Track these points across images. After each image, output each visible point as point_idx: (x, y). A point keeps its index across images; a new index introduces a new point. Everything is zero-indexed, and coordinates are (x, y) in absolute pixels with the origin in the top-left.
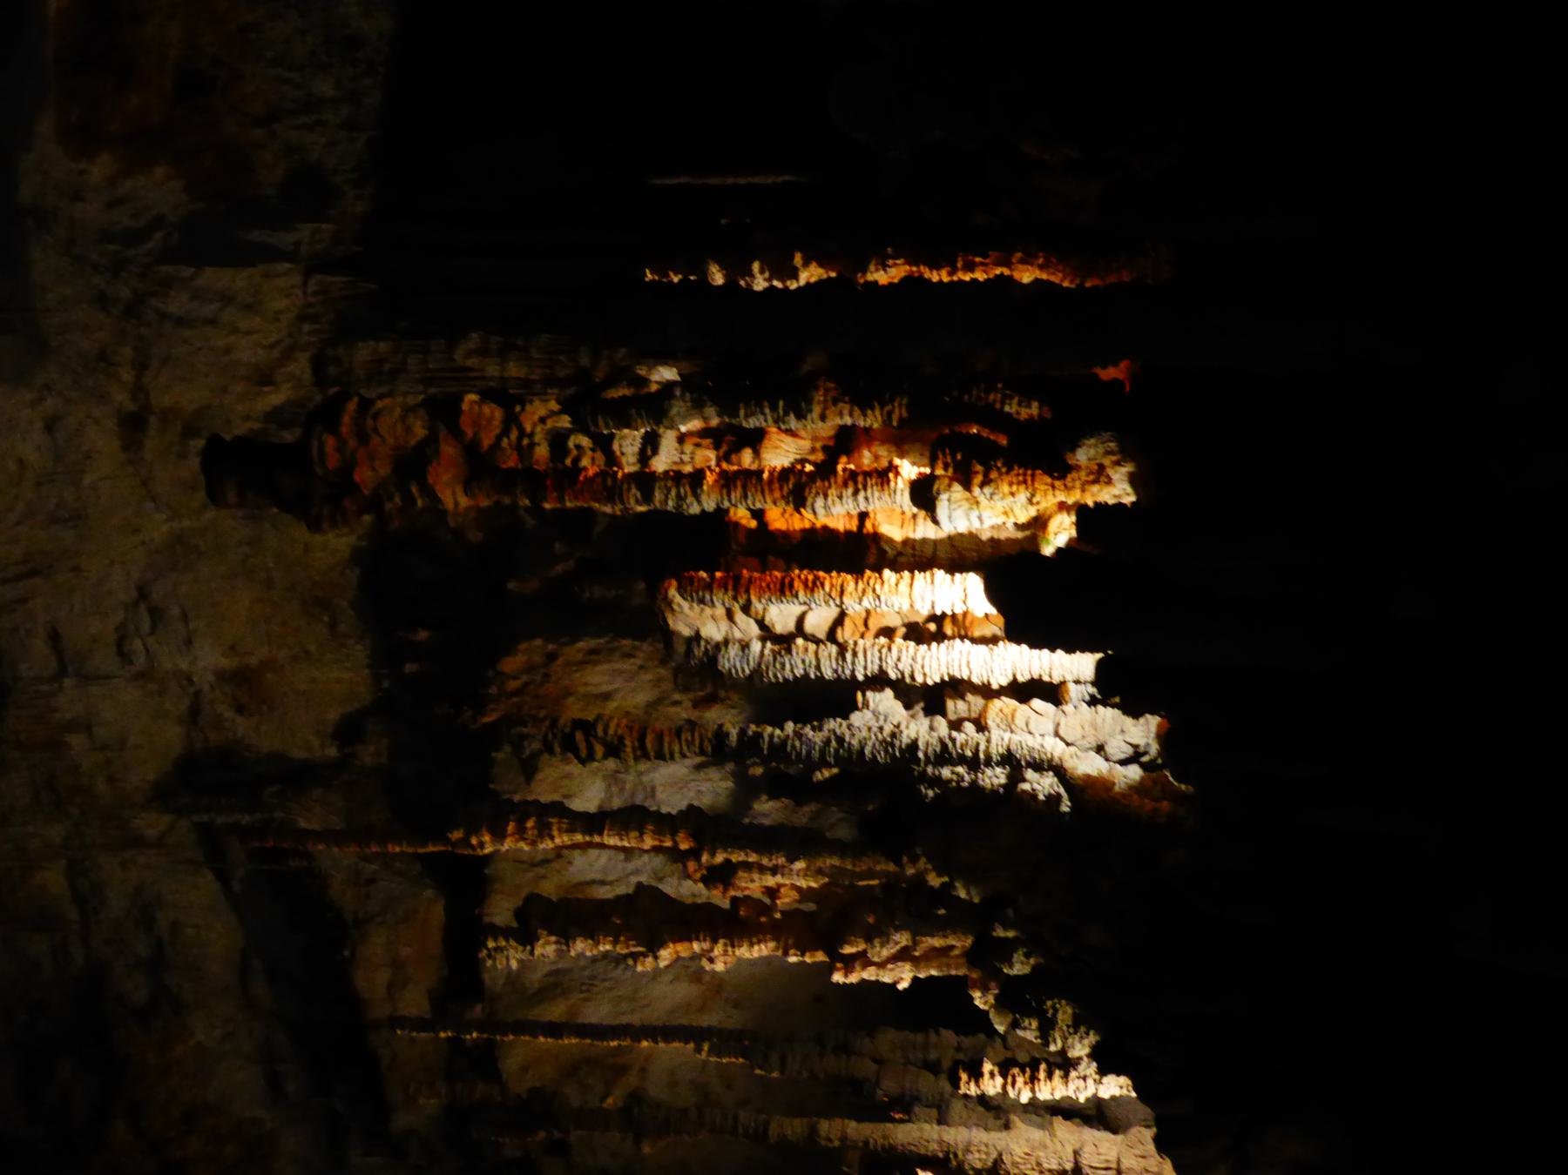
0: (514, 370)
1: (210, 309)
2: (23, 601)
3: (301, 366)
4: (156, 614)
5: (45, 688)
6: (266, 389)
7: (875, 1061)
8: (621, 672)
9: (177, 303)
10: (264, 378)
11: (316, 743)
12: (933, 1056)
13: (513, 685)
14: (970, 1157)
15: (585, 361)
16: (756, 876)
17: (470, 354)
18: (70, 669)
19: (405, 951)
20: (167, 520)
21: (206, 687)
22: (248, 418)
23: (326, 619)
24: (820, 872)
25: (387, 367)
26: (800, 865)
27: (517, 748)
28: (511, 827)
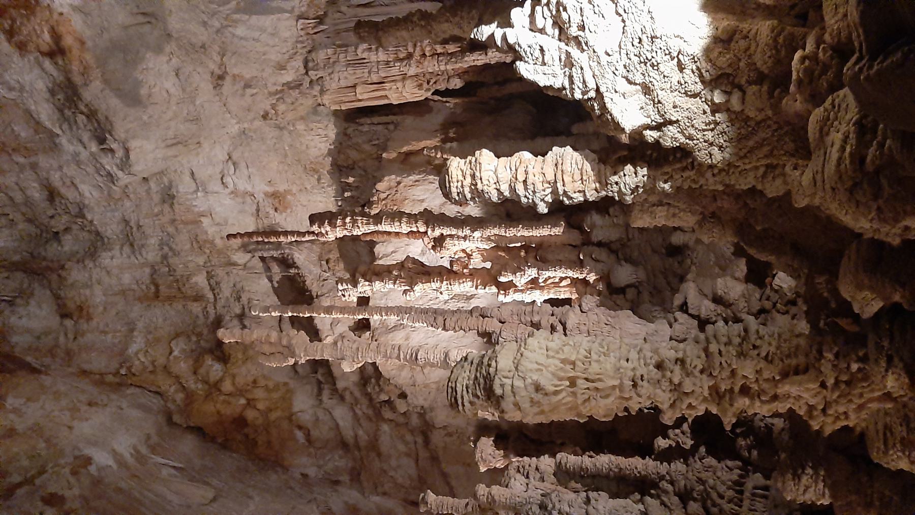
1: (256, 34)
2: (176, 156)
3: (298, 63)
4: (234, 164)
5: (189, 197)
7: (501, 322)
8: (428, 190)
9: (240, 31)
10: (282, 67)
12: (536, 319)
13: (383, 196)
15: (411, 50)
16: (456, 242)
17: (364, 51)
20: (237, 123)
21: (261, 201)
22: (275, 84)
23: (316, 177)
24: (489, 239)
25: (331, 60)
26: (477, 234)
28: (339, 222)
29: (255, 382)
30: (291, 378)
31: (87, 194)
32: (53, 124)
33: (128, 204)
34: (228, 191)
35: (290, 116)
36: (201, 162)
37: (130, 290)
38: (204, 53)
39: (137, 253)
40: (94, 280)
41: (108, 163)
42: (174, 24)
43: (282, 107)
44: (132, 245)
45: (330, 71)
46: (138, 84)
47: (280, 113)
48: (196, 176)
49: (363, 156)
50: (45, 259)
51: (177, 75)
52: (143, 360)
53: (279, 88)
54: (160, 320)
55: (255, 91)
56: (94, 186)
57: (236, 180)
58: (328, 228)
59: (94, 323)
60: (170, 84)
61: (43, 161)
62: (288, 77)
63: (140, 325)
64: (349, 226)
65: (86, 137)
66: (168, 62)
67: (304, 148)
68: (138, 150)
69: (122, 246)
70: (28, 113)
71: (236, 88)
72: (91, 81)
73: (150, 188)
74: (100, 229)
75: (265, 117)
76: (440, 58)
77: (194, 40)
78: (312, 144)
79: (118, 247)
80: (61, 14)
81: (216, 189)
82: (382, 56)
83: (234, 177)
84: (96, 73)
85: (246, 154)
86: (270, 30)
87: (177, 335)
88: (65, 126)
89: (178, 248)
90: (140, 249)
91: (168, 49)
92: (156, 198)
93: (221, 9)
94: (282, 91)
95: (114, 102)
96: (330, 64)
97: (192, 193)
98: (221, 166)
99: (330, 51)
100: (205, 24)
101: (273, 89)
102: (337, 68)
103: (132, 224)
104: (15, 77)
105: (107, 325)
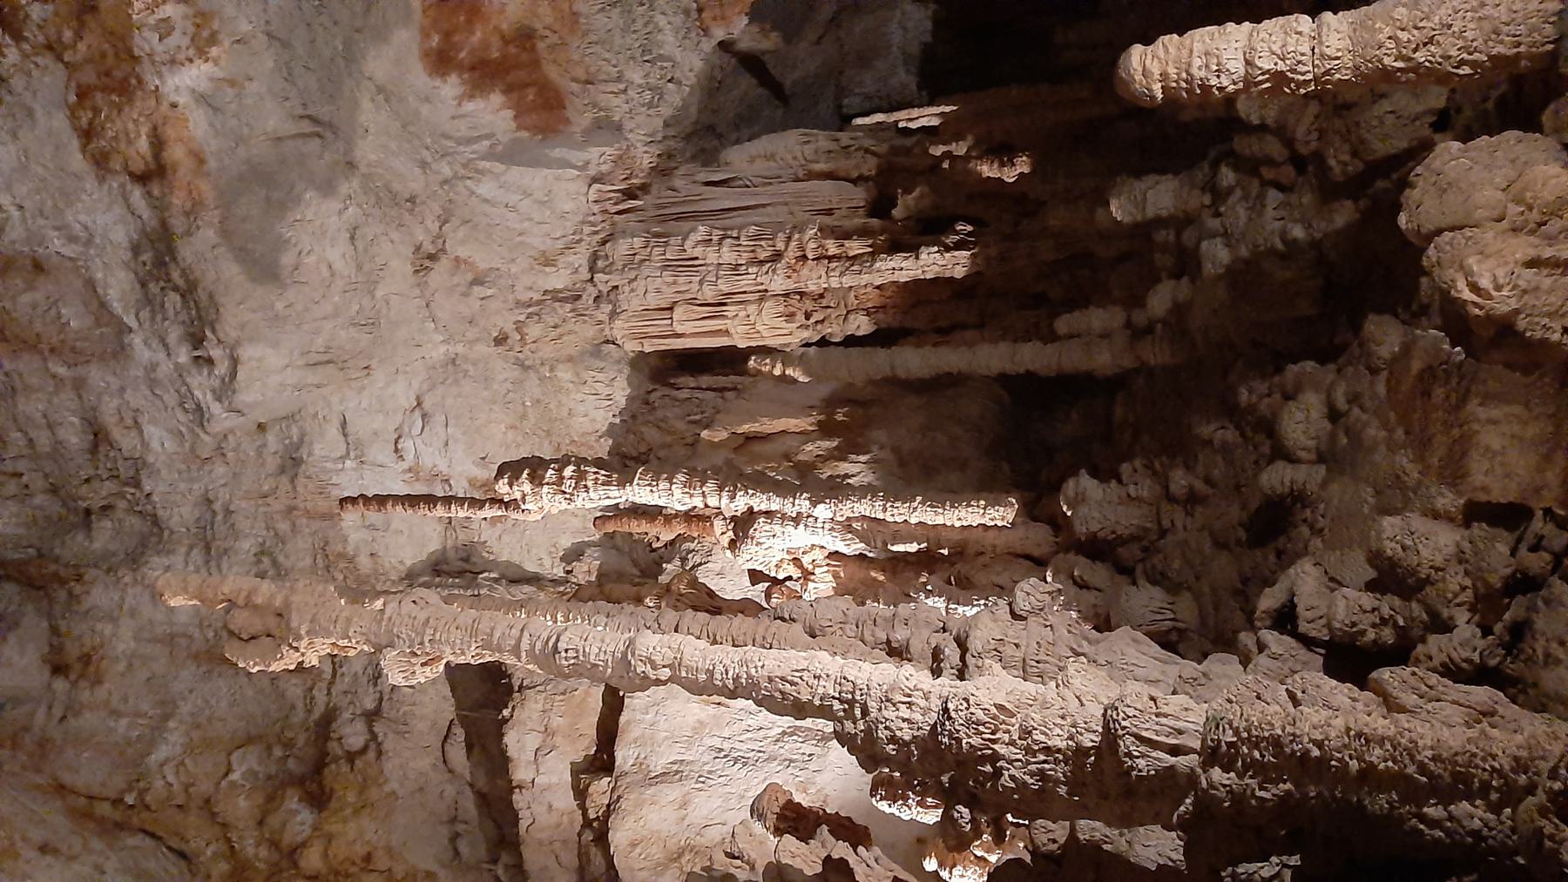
0: (728, 255)
1: (513, 198)
3: (580, 258)
4: (424, 416)
6: (547, 269)
9: (486, 188)
10: (547, 261)
11: (547, 563)
12: (900, 635)
14: (889, 713)
15: (780, 246)
16: (777, 528)
18: (352, 455)
19: (556, 722)
24: (847, 526)
26: (823, 511)
27: (684, 560)
29: (368, 858)
30: (443, 866)
31: (155, 445)
32: (125, 308)
33: (220, 469)
34: (405, 465)
35: (547, 351)
36: (364, 405)
37: (184, 635)
38: (411, 211)
39: (213, 563)
40: (125, 608)
41: (201, 385)
42: (367, 151)
43: (534, 331)
44: (208, 548)
45: (632, 275)
46: (282, 244)
47: (529, 339)
48: (350, 429)
49: (668, 439)
50: (57, 560)
51: (352, 238)
52: (171, 778)
53: (537, 297)
54: (224, 704)
55: (490, 292)
56: (170, 431)
57: (421, 447)
58: (527, 487)
59: (101, 693)
60: (337, 254)
61: (97, 376)
62: (558, 279)
63: (185, 708)
64: (568, 485)
65: (174, 334)
66: (340, 213)
67: (565, 413)
68: (254, 364)
69: (191, 548)
70: (91, 284)
71: (456, 280)
72: (198, 228)
73: (265, 445)
74: (160, 513)
75: (501, 340)
76: (833, 265)
77: (396, 186)
78: (581, 408)
79: (183, 550)
80: (174, 106)
81: (381, 459)
82: (728, 255)
83: (418, 441)
84: (213, 215)
85: (449, 401)
86: (539, 195)
87: (249, 740)
88: (145, 314)
89: (287, 564)
90: (220, 557)
91: (344, 189)
92: (272, 463)
93: (462, 148)
94: (539, 302)
95: (231, 270)
96: (634, 262)
97: (335, 461)
98: (399, 418)
99: (638, 242)
100: (424, 165)
101: (525, 296)
102: (646, 272)
103: (217, 506)
104: (82, 218)
105: (125, 700)
